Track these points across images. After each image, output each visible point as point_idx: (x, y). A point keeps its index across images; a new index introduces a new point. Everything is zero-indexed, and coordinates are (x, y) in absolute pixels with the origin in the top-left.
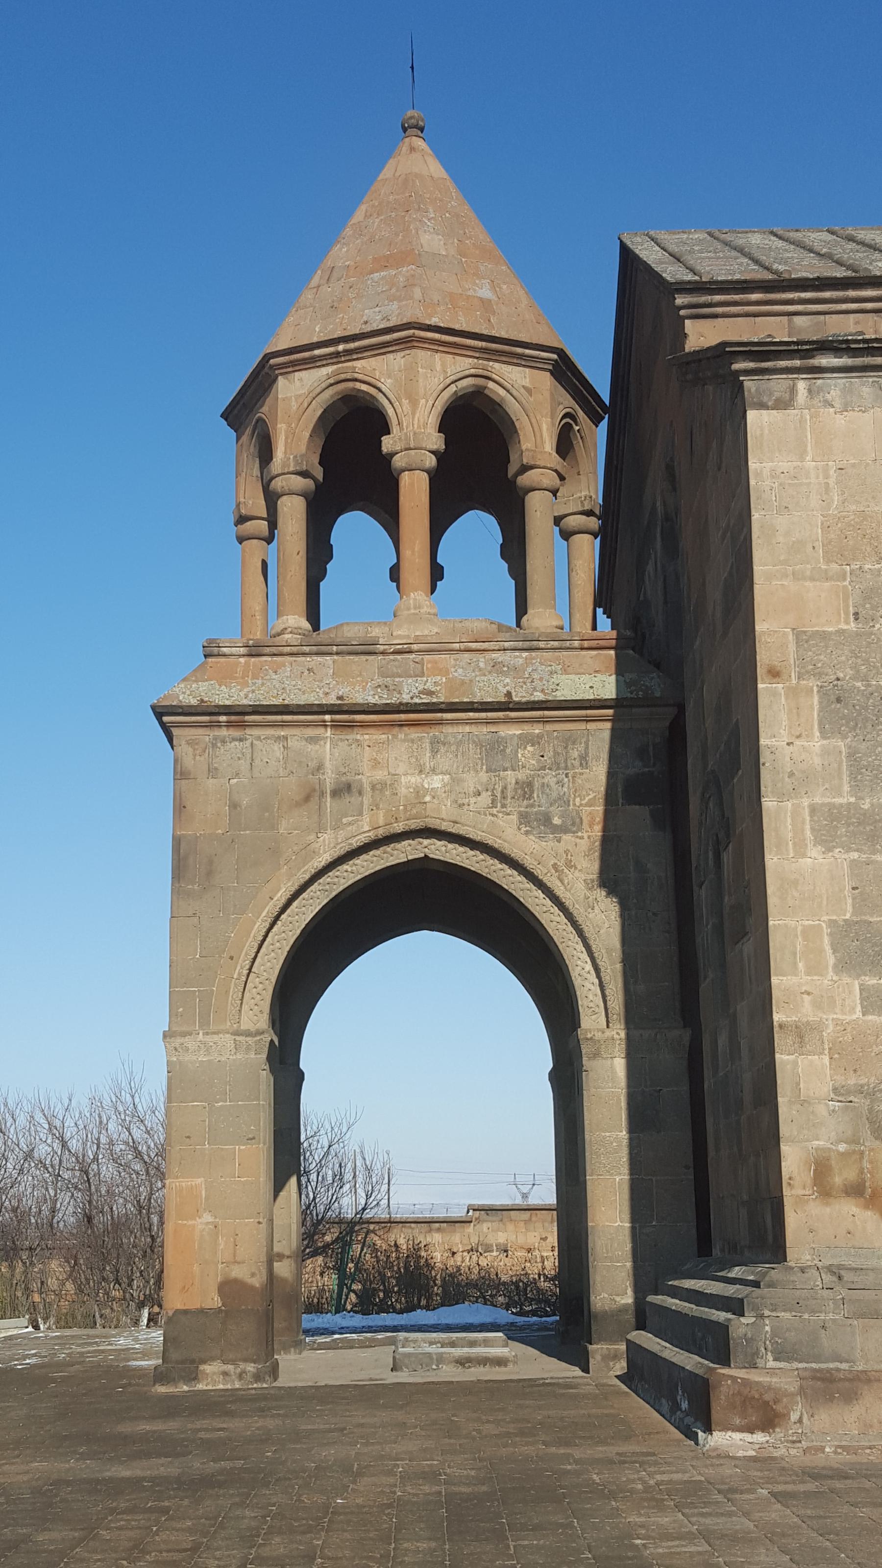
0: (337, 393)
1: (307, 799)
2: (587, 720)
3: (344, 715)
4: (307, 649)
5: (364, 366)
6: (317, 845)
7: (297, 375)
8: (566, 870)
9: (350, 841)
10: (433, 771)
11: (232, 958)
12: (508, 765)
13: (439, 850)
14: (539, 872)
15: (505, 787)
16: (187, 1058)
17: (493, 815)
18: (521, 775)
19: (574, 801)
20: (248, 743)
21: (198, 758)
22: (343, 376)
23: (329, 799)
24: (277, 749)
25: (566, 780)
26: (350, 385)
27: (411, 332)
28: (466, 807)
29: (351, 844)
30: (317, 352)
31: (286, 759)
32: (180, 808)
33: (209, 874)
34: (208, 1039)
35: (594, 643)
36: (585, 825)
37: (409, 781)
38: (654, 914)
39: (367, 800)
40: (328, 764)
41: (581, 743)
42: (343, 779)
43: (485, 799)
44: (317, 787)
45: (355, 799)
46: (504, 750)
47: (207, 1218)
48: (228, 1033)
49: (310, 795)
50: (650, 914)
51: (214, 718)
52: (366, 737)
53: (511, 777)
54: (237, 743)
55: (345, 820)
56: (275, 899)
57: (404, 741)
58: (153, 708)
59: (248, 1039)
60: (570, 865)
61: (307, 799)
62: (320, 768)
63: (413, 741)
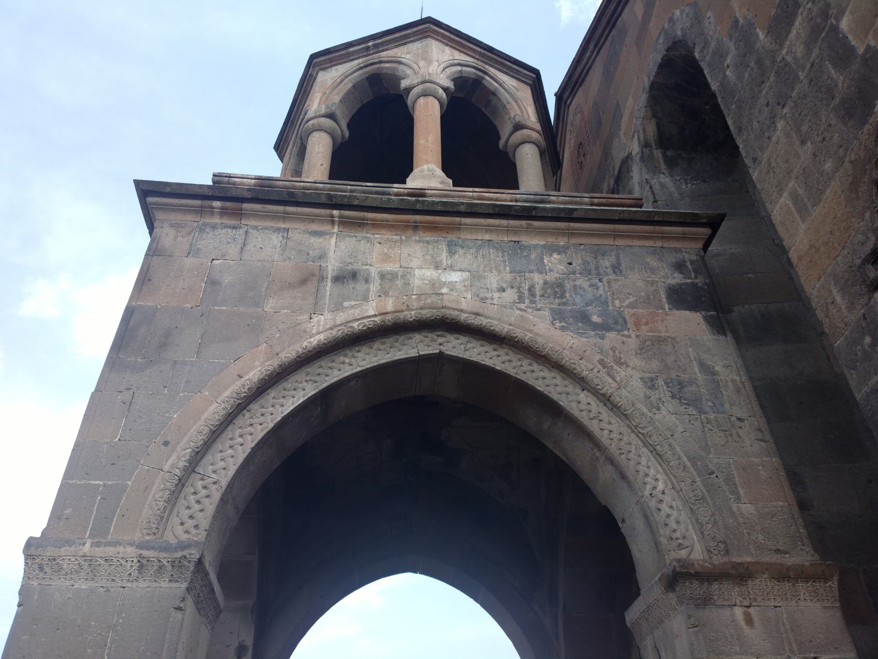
0: (366, 73)
2: (615, 236)
6: (310, 325)
7: (334, 68)
8: (615, 367)
9: (350, 325)
10: (452, 268)
11: (166, 444)
12: (533, 268)
13: (457, 347)
14: (583, 368)
15: (531, 289)
17: (520, 310)
19: (613, 302)
20: (242, 231)
21: (179, 239)
23: (329, 284)
24: (276, 239)
25: (600, 284)
26: (377, 66)
27: (427, 25)
28: (489, 301)
29: (351, 327)
30: (351, 49)
31: (284, 248)
33: (163, 346)
38: (740, 420)
39: (374, 287)
40: (331, 254)
41: (610, 255)
42: (350, 267)
43: (510, 295)
44: (317, 272)
45: (360, 286)
46: (528, 256)
50: (733, 419)
51: (207, 203)
53: (538, 279)
54: (229, 230)
55: (346, 304)
57: (419, 241)
58: (138, 183)
60: (619, 362)
61: (304, 282)
62: (322, 256)
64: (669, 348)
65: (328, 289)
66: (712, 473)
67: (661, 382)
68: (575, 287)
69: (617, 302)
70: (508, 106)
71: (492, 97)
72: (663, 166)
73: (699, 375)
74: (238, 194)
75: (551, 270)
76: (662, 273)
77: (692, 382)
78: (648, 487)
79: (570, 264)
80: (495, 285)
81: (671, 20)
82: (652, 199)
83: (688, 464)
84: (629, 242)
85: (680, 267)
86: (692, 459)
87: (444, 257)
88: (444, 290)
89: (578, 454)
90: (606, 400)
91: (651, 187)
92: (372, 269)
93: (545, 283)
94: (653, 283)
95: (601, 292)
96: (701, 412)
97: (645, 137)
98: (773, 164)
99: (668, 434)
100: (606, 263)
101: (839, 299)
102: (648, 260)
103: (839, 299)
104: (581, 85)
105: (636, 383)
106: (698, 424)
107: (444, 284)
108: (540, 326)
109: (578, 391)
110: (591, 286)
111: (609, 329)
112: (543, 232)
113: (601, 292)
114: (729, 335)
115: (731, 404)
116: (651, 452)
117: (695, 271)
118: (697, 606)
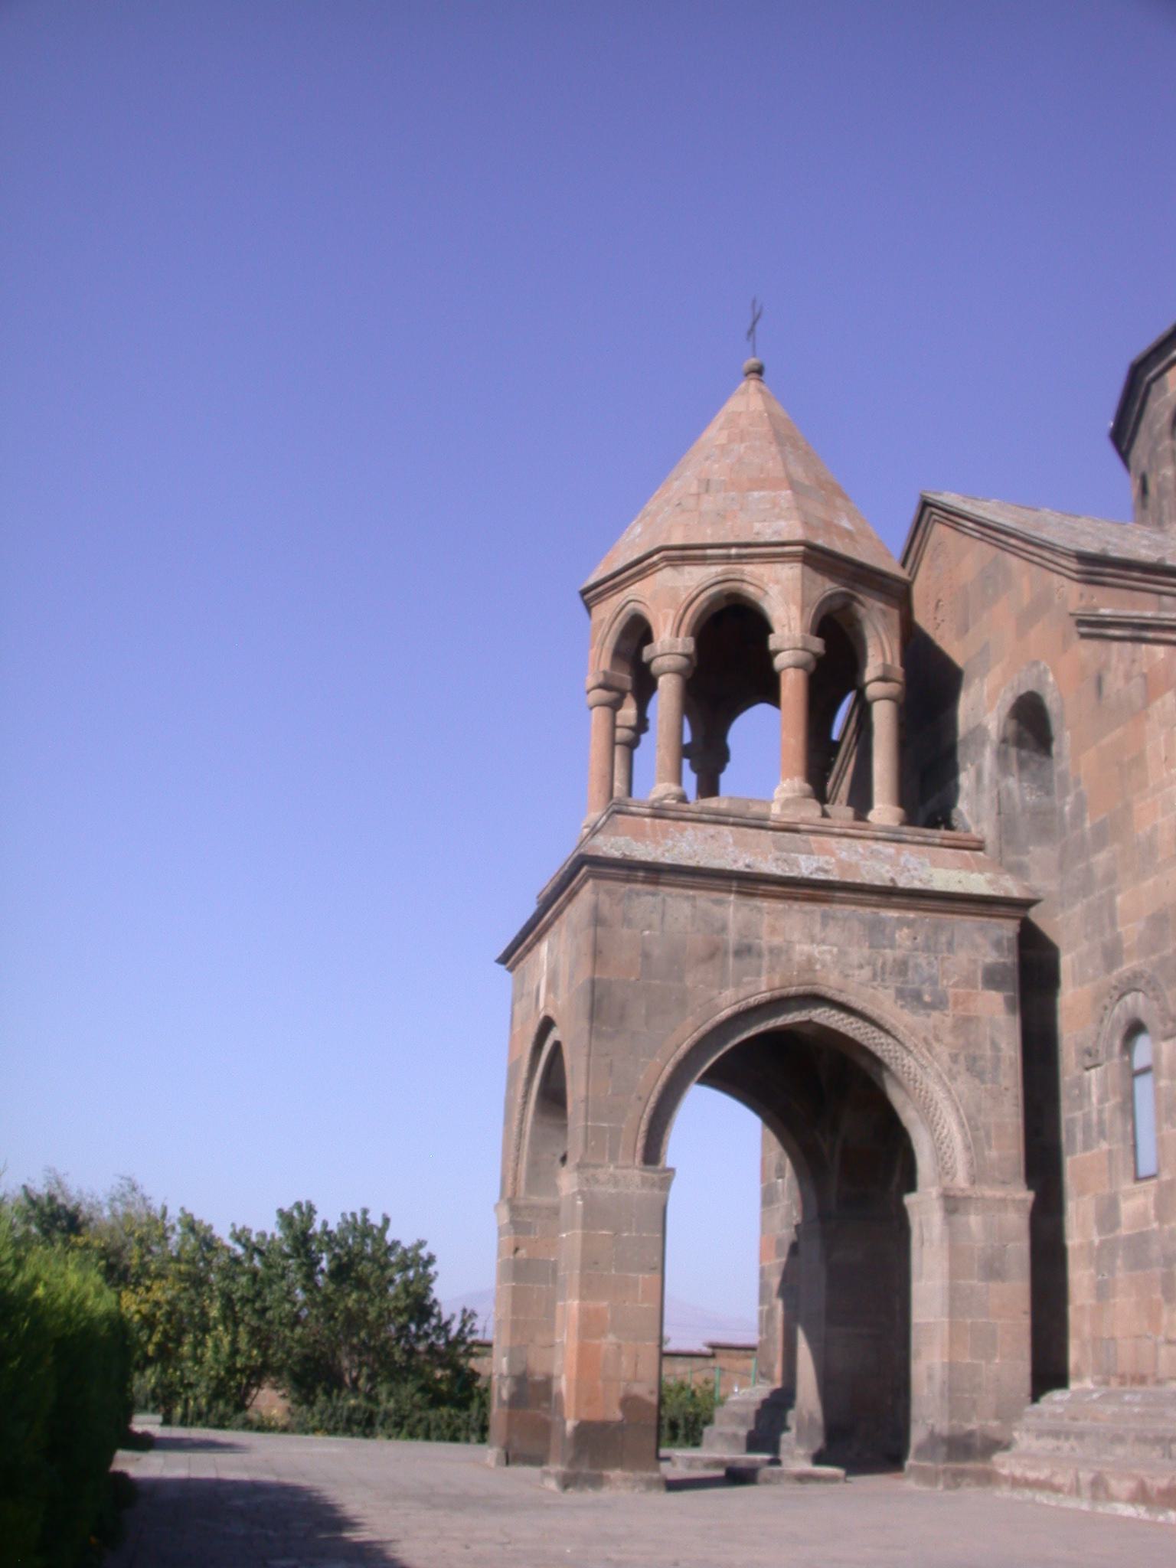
1: (712, 956)
3: (749, 883)
4: (705, 817)
5: (751, 570)
10: (823, 942)
12: (885, 942)
15: (884, 964)
16: (596, 1188)
18: (899, 953)
20: (659, 898)
22: (731, 576)
24: (686, 908)
26: (737, 585)
30: (709, 552)
32: (597, 953)
34: (618, 1172)
35: (952, 842)
36: (950, 1005)
37: (803, 949)
39: (766, 962)
40: (732, 927)
42: (745, 941)
43: (867, 972)
47: (611, 1338)
49: (714, 953)
52: (765, 904)
55: (745, 979)
60: (937, 1039)
61: (712, 956)
62: (724, 928)
63: (805, 913)
67: (962, 1058)
80: (856, 963)
85: (997, 945)
86: (969, 1119)
87: (817, 929)
88: (818, 967)
93: (895, 960)
94: (975, 962)
96: (983, 1082)
105: (945, 1058)
108: (883, 1003)
112: (897, 907)
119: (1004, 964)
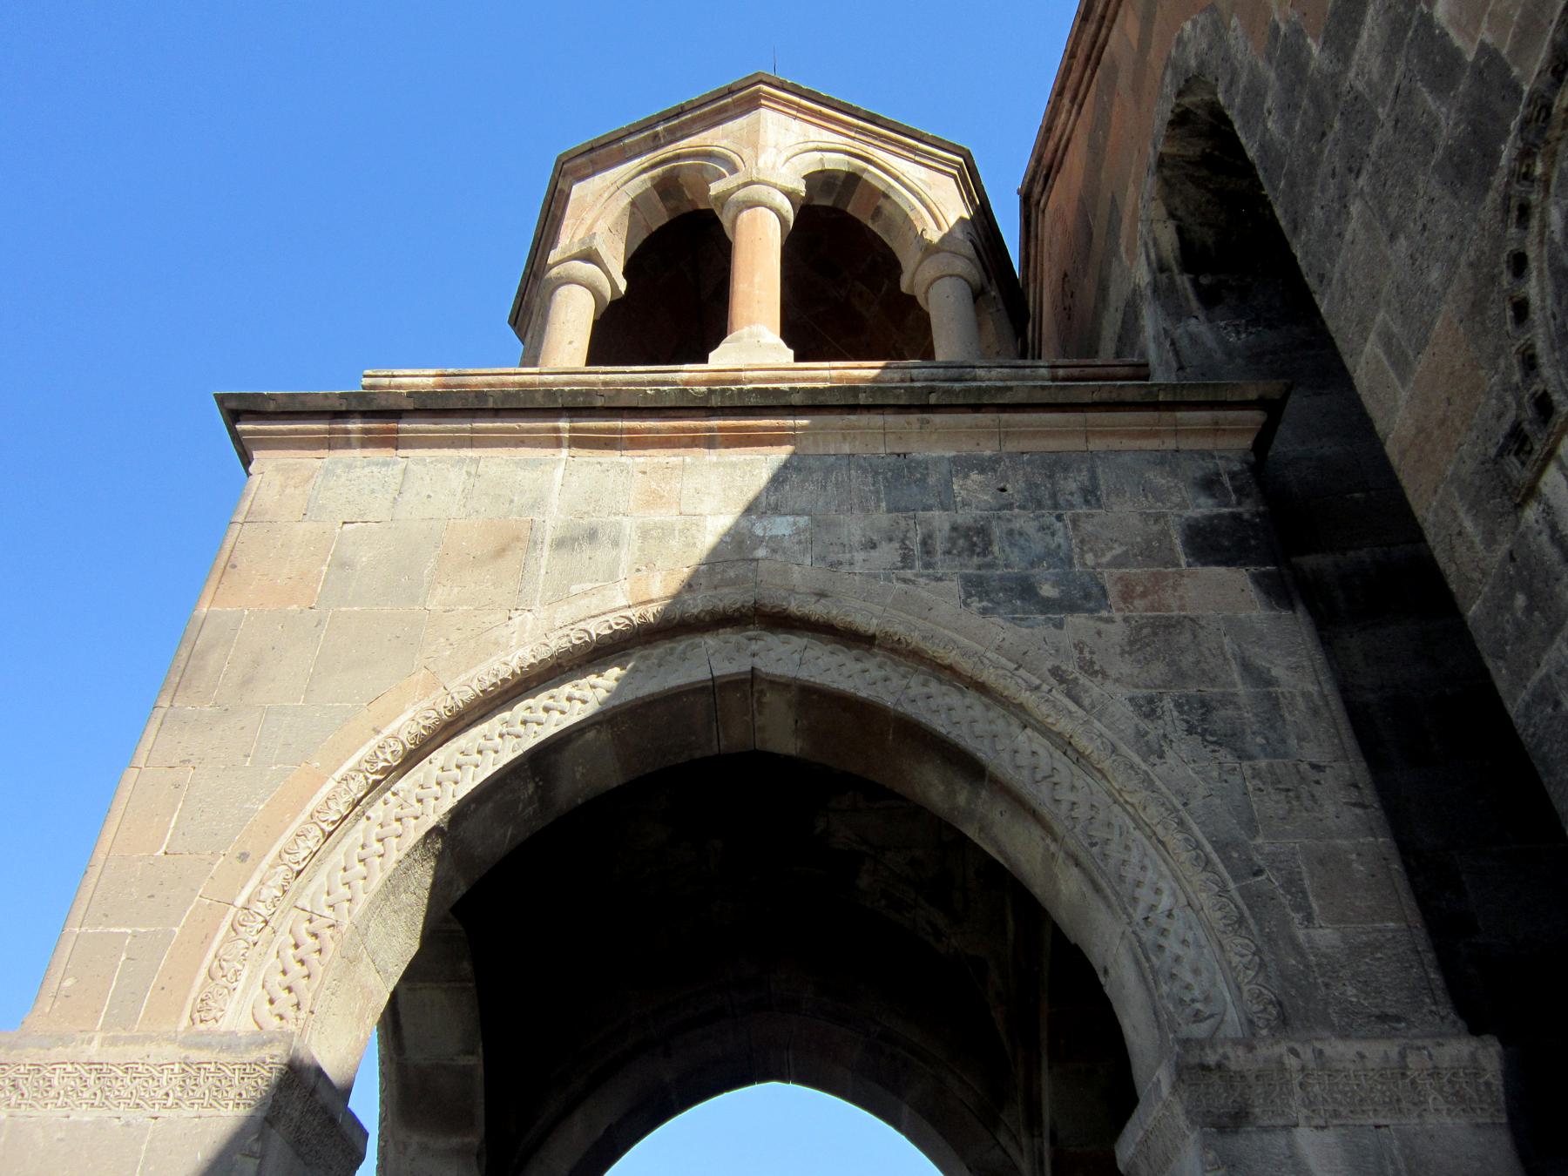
0: (653, 179)
2: (1087, 435)
8: (1083, 680)
9: (582, 625)
13: (783, 657)
15: (926, 543)
17: (905, 581)
18: (965, 517)
19: (1082, 557)
21: (288, 491)
25: (1059, 525)
28: (845, 568)
33: (247, 682)
38: (1315, 767)
40: (554, 501)
41: (1080, 470)
42: (585, 521)
43: (888, 554)
45: (603, 555)
46: (923, 479)
48: (172, 1041)
50: (1304, 767)
53: (940, 520)
54: (375, 469)
55: (575, 589)
56: (386, 732)
58: (221, 399)
59: (225, 1057)
60: (1088, 668)
61: (501, 552)
62: (538, 504)
64: (1185, 639)
65: (544, 562)
66: (1259, 872)
68: (1011, 532)
69: (1090, 558)
70: (912, 215)
71: (881, 201)
72: (1194, 303)
73: (1240, 687)
74: (392, 404)
75: (965, 504)
76: (1176, 499)
77: (1228, 700)
78: (1142, 906)
79: (1003, 490)
80: (857, 537)
81: (1180, 41)
82: (1175, 365)
83: (1214, 856)
84: (1115, 443)
85: (1209, 485)
86: (1222, 847)
88: (761, 553)
89: (1019, 847)
90: (1064, 744)
91: (1173, 343)
92: (626, 521)
93: (954, 528)
94: (1158, 518)
95: (1059, 539)
96: (1242, 755)
97: (1157, 254)
98: (1351, 283)
99: (1177, 803)
100: (1071, 484)
101: (1469, 525)
102: (1150, 475)
103: (1469, 525)
104: (1058, 172)
105: (1123, 711)
106: (1237, 779)
107: (761, 540)
109: (1015, 728)
110: (1042, 528)
111: (1072, 608)
113: (1059, 539)
114: (1300, 608)
115: (1300, 739)
116: (1149, 838)
117: (1237, 490)
118: (1222, 1129)
119: (1236, 517)
